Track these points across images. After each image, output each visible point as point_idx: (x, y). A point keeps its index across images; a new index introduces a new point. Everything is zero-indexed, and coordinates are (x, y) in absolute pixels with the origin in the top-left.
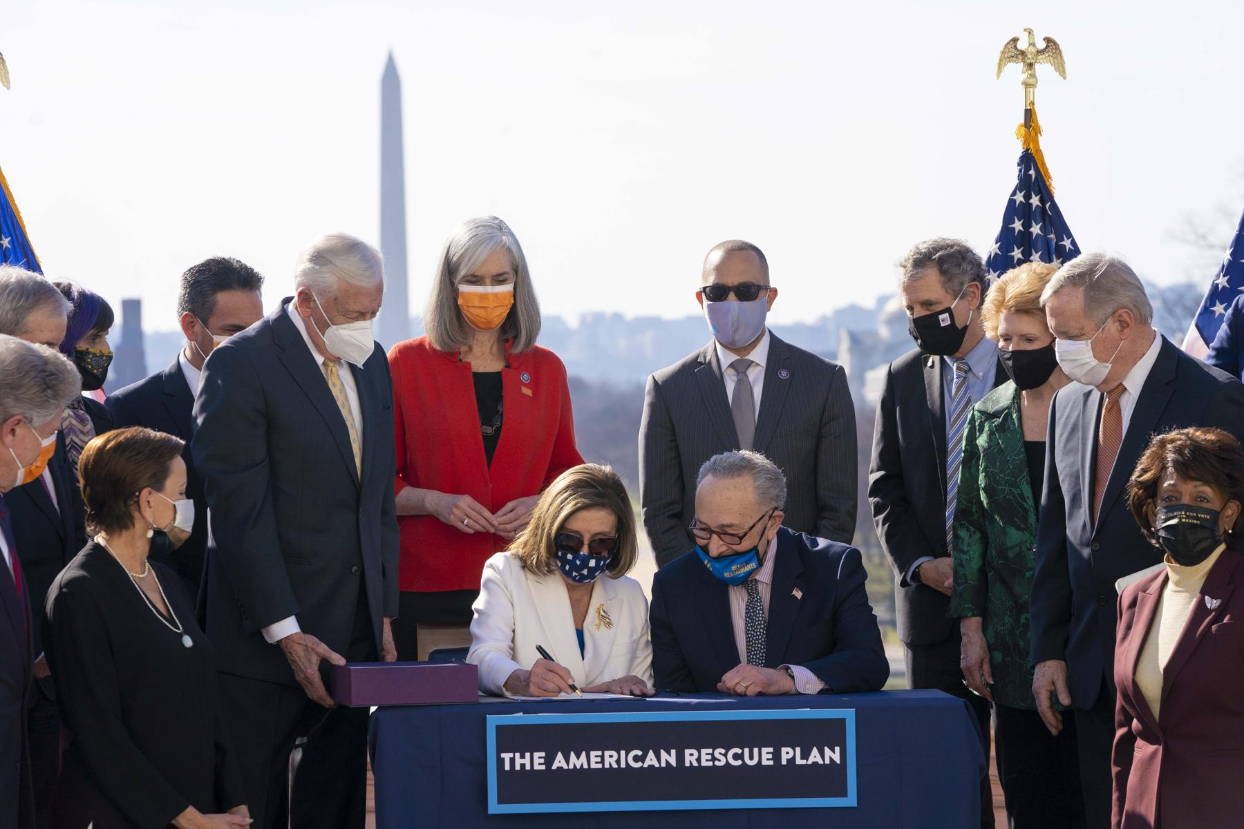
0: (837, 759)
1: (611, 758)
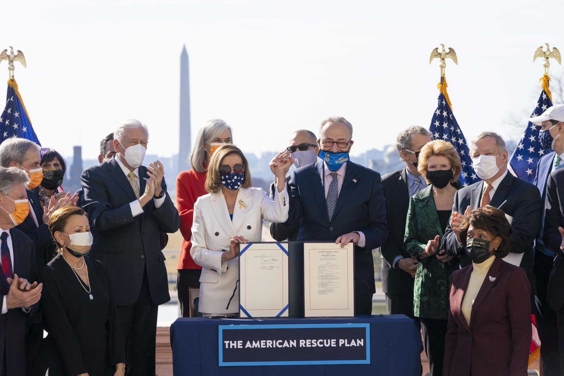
0: (362, 344)
1: (269, 343)
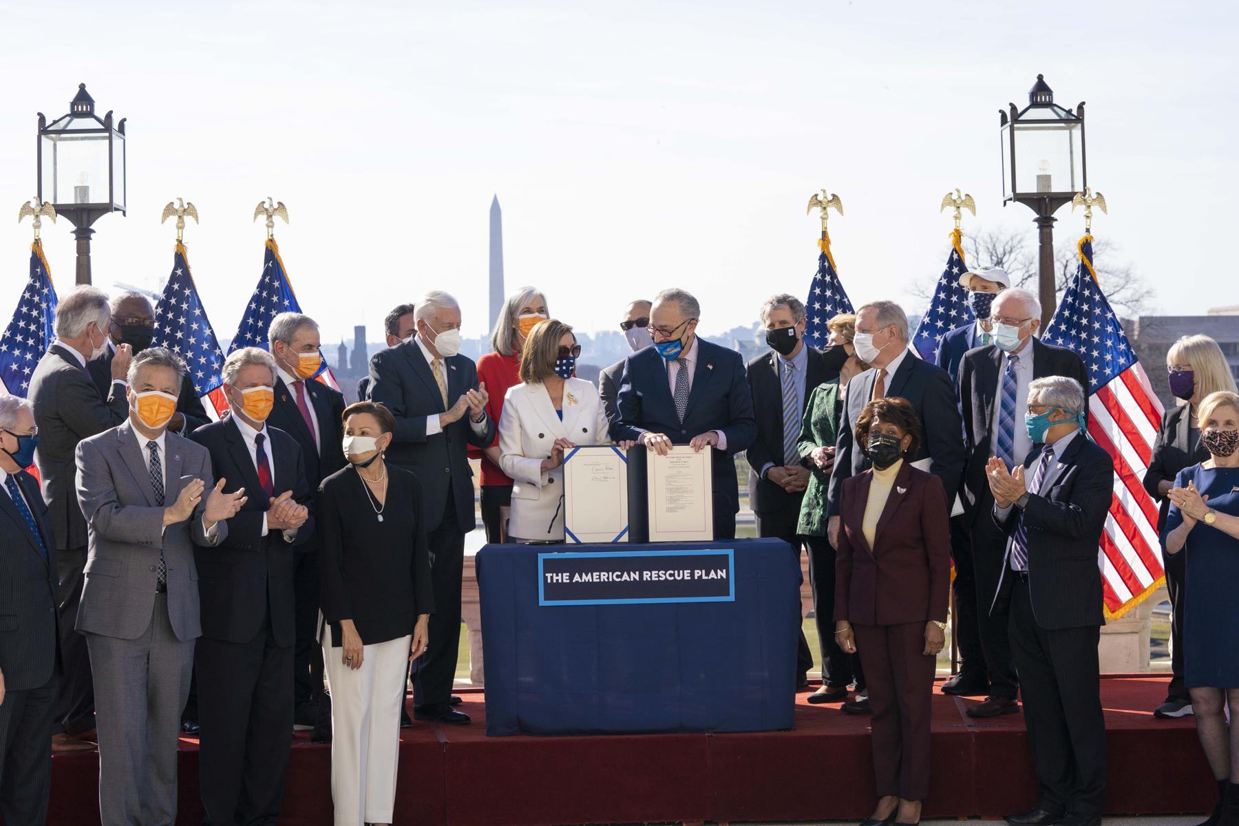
1: (604, 576)
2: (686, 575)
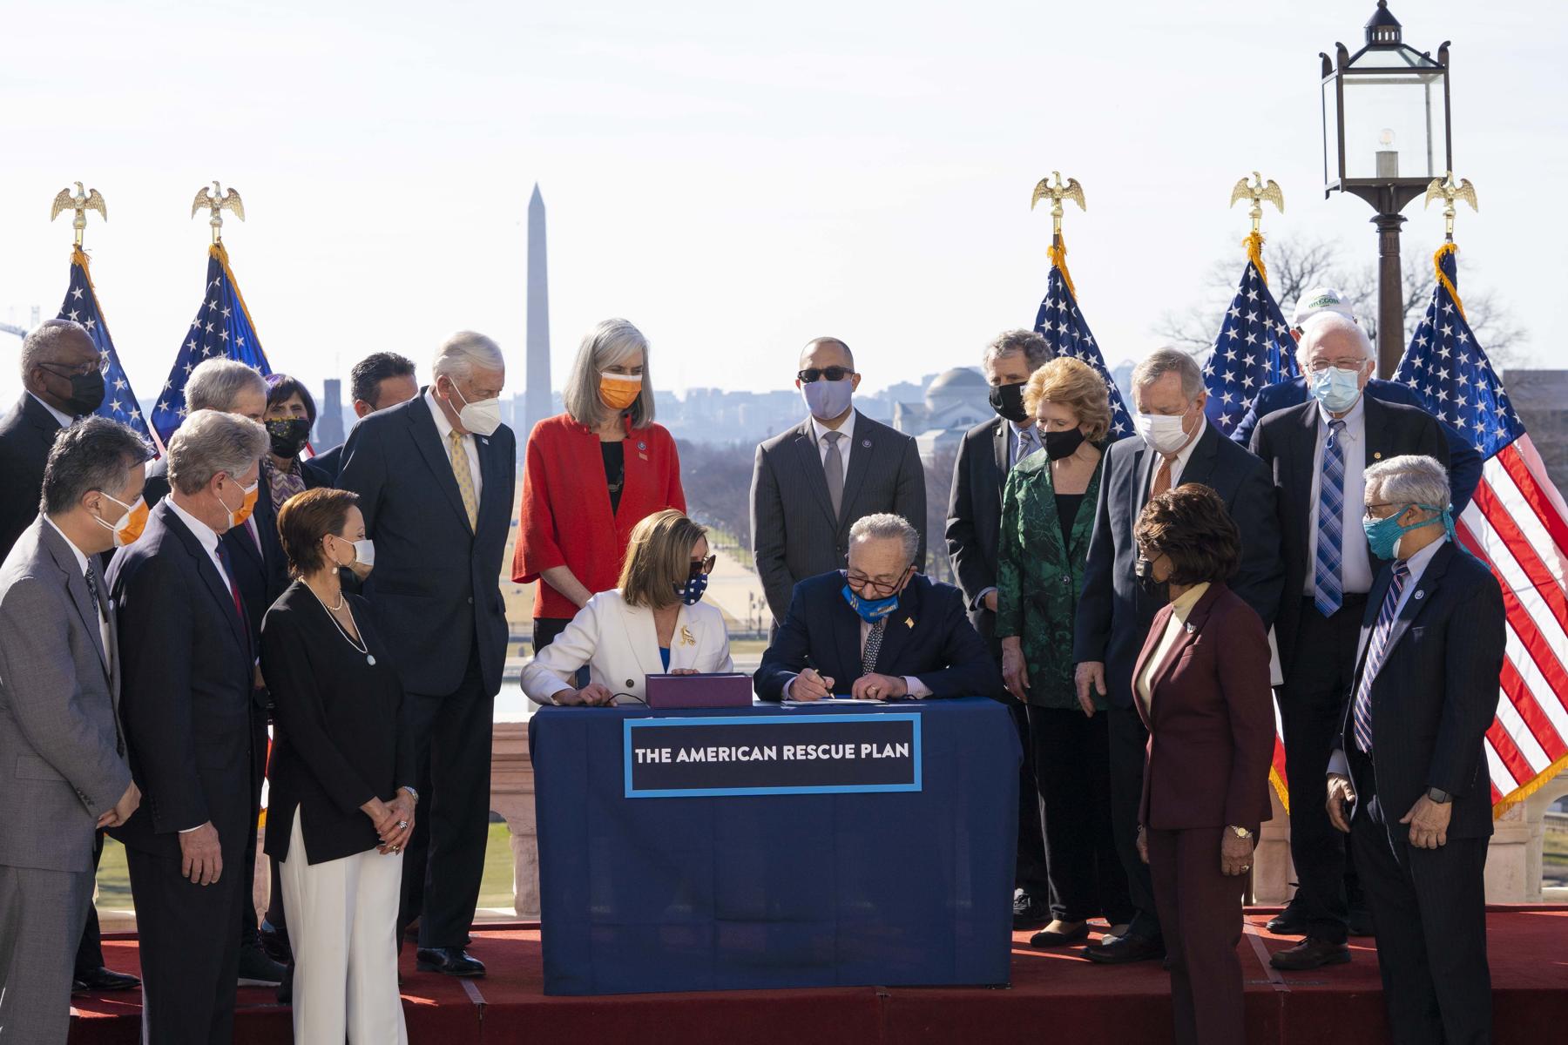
0: (906, 753)
1: (724, 753)
2: (849, 751)
